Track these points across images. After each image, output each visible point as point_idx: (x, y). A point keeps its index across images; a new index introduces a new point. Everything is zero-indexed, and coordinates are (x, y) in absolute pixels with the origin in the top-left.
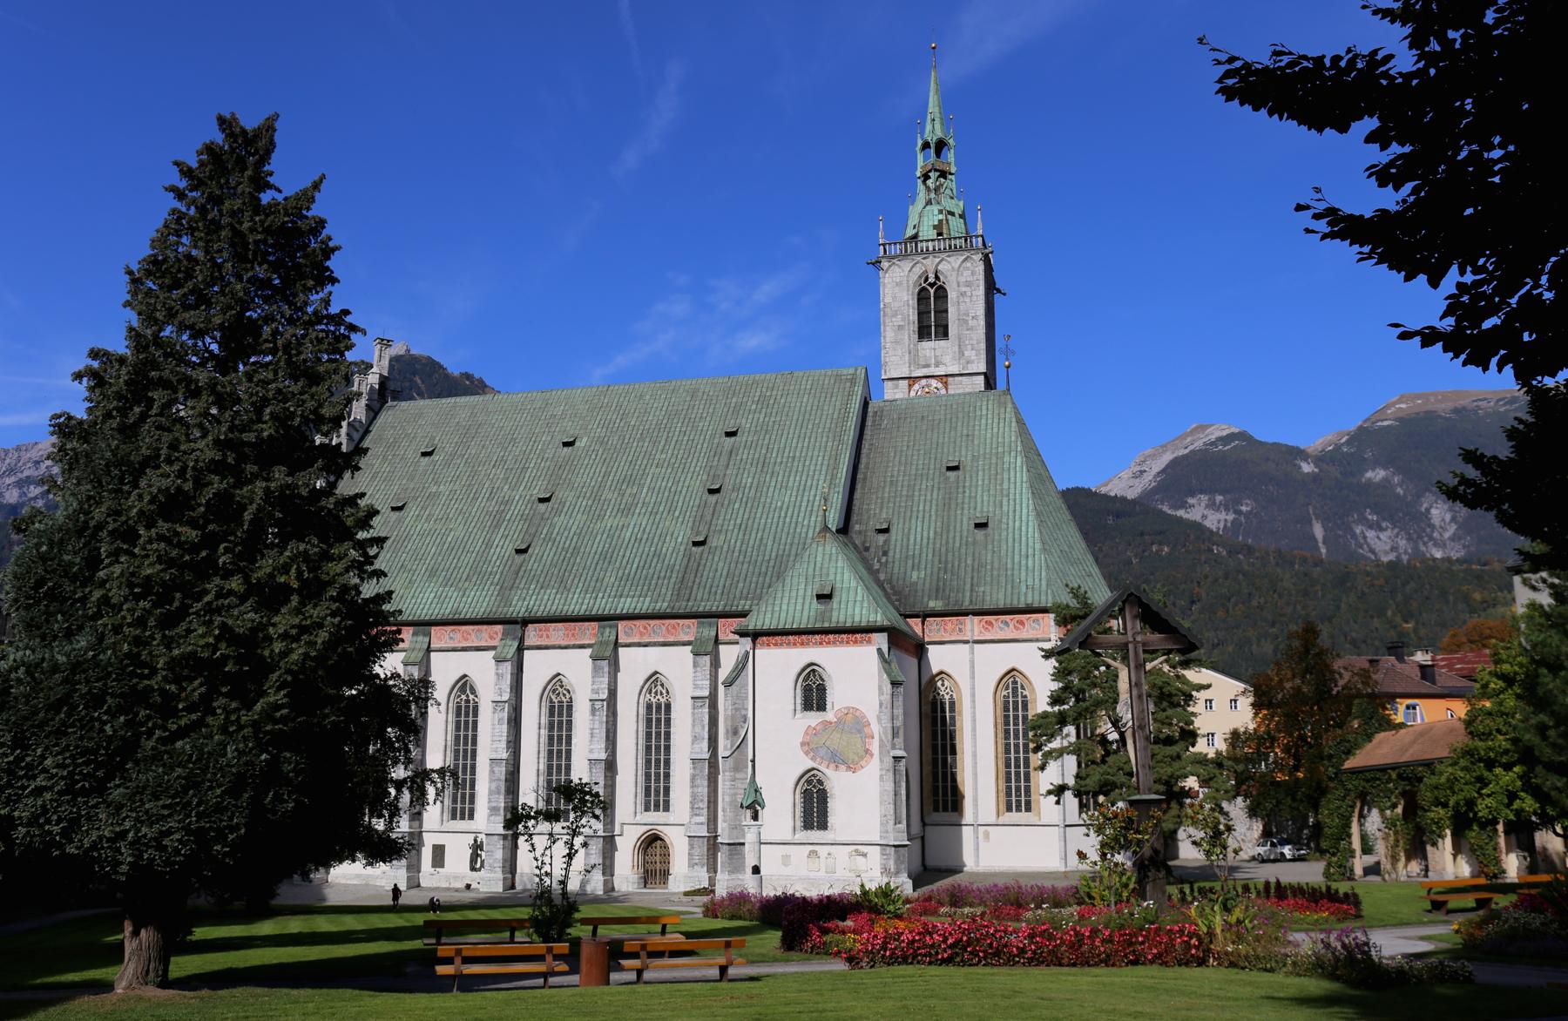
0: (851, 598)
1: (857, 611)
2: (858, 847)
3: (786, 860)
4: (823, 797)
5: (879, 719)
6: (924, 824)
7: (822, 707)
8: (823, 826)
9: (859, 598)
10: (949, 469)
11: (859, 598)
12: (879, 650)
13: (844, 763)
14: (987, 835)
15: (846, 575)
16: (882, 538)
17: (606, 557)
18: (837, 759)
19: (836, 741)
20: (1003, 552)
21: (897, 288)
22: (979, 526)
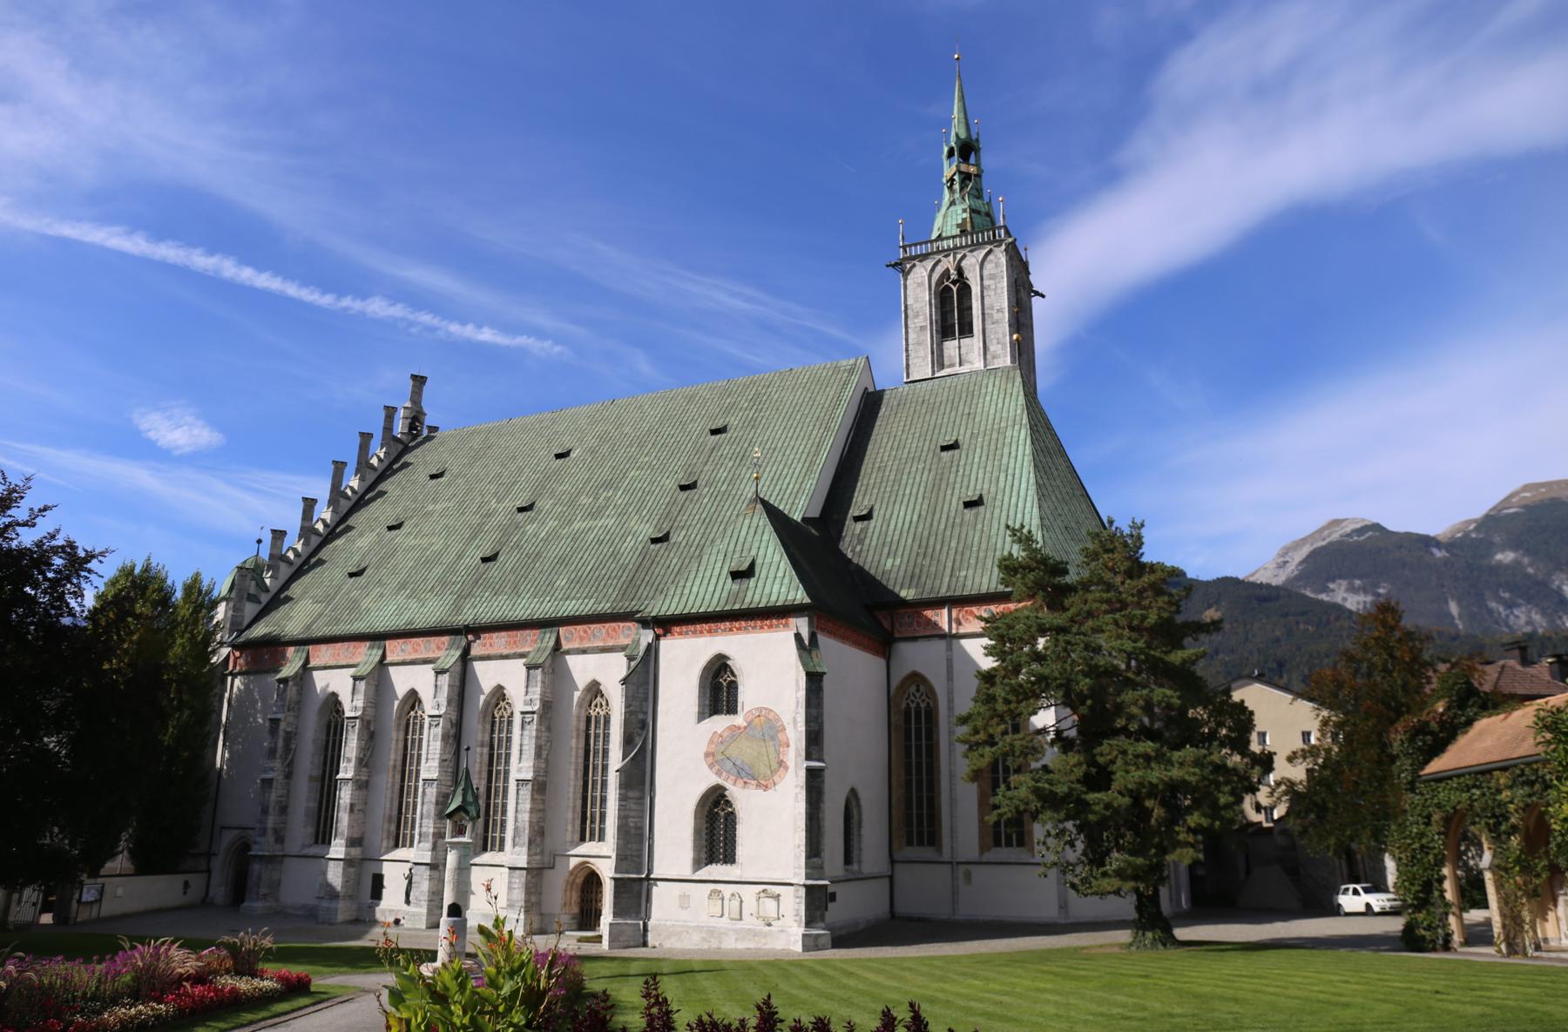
0: (771, 575)
1: (775, 590)
2: (767, 886)
3: (684, 901)
4: (731, 820)
6: (893, 862)
7: (732, 709)
8: (730, 858)
9: (780, 574)
10: (944, 448)
11: (780, 574)
12: (798, 637)
14: (968, 876)
15: (770, 550)
16: (859, 525)
17: (563, 561)
18: (746, 774)
19: (744, 751)
20: (994, 531)
21: (918, 290)
22: (969, 505)
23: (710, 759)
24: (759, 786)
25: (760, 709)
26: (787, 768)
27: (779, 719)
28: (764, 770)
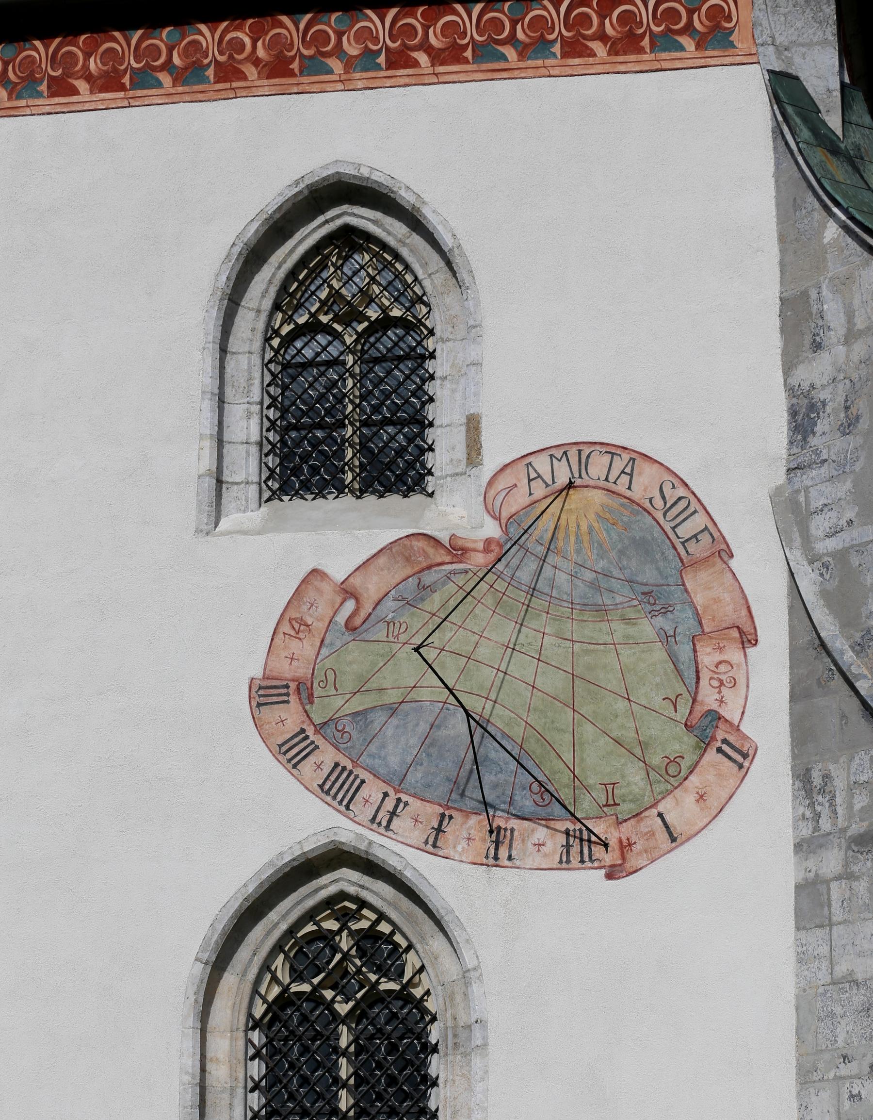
5: (792, 514)
7: (397, 467)
12: (785, 90)
13: (550, 802)
18: (505, 788)
19: (508, 663)
23: (289, 717)
24: (581, 846)
25: (580, 452)
26: (741, 755)
27: (688, 503)
28: (599, 762)
